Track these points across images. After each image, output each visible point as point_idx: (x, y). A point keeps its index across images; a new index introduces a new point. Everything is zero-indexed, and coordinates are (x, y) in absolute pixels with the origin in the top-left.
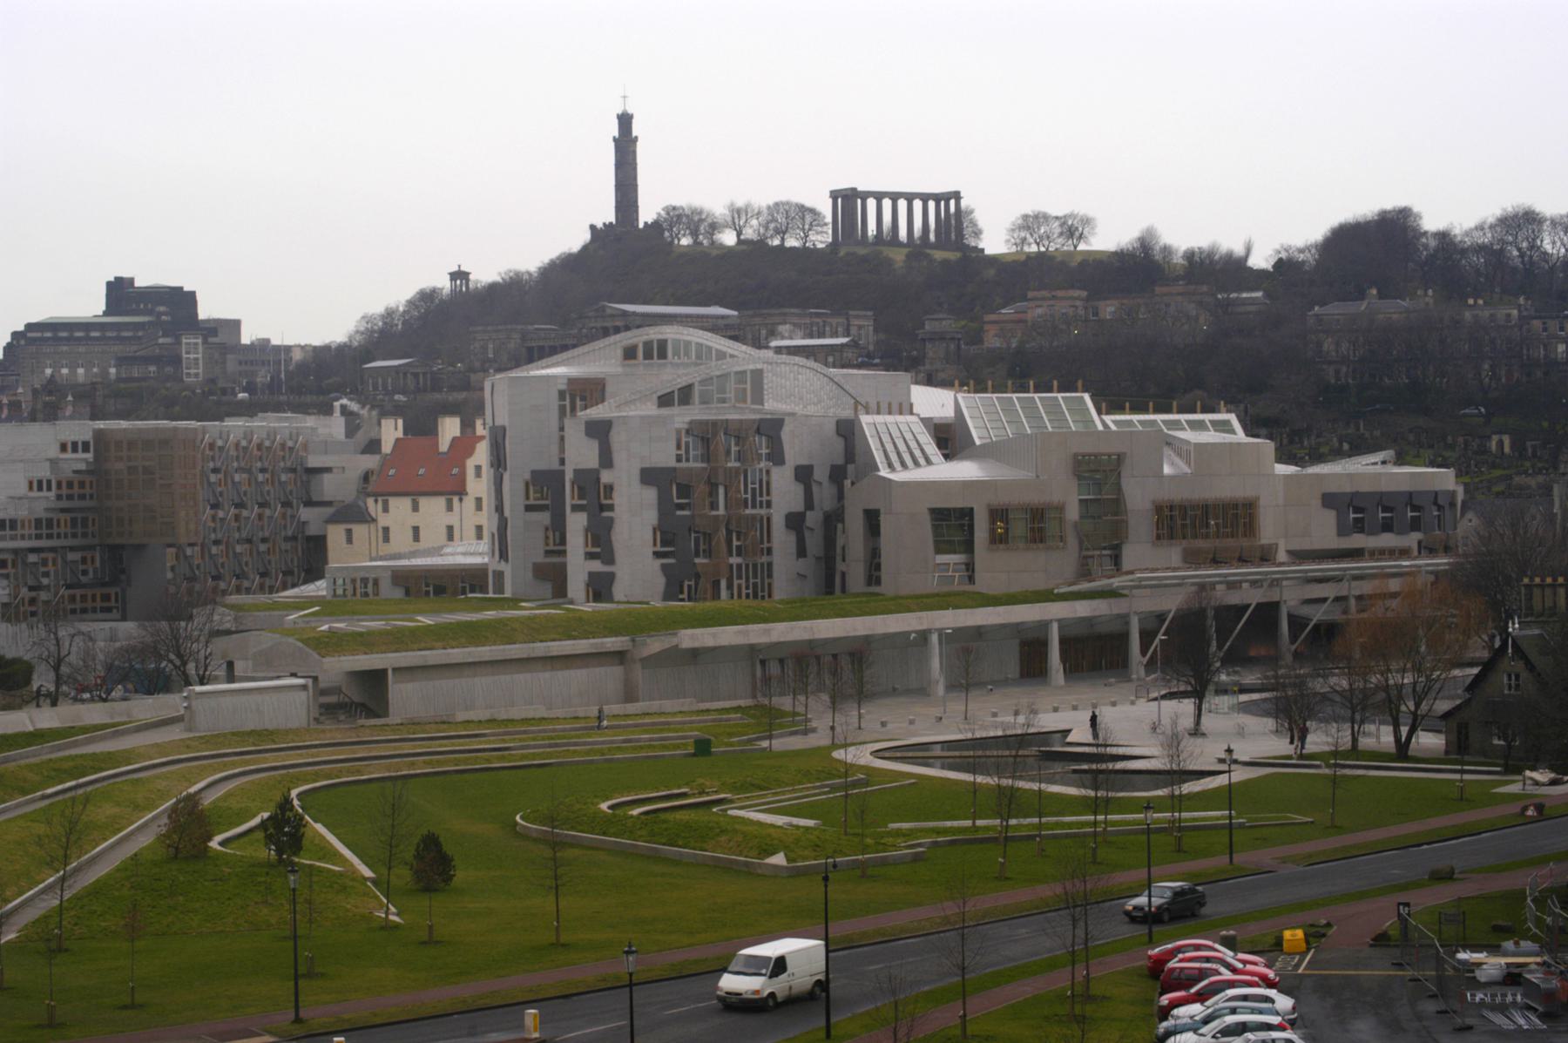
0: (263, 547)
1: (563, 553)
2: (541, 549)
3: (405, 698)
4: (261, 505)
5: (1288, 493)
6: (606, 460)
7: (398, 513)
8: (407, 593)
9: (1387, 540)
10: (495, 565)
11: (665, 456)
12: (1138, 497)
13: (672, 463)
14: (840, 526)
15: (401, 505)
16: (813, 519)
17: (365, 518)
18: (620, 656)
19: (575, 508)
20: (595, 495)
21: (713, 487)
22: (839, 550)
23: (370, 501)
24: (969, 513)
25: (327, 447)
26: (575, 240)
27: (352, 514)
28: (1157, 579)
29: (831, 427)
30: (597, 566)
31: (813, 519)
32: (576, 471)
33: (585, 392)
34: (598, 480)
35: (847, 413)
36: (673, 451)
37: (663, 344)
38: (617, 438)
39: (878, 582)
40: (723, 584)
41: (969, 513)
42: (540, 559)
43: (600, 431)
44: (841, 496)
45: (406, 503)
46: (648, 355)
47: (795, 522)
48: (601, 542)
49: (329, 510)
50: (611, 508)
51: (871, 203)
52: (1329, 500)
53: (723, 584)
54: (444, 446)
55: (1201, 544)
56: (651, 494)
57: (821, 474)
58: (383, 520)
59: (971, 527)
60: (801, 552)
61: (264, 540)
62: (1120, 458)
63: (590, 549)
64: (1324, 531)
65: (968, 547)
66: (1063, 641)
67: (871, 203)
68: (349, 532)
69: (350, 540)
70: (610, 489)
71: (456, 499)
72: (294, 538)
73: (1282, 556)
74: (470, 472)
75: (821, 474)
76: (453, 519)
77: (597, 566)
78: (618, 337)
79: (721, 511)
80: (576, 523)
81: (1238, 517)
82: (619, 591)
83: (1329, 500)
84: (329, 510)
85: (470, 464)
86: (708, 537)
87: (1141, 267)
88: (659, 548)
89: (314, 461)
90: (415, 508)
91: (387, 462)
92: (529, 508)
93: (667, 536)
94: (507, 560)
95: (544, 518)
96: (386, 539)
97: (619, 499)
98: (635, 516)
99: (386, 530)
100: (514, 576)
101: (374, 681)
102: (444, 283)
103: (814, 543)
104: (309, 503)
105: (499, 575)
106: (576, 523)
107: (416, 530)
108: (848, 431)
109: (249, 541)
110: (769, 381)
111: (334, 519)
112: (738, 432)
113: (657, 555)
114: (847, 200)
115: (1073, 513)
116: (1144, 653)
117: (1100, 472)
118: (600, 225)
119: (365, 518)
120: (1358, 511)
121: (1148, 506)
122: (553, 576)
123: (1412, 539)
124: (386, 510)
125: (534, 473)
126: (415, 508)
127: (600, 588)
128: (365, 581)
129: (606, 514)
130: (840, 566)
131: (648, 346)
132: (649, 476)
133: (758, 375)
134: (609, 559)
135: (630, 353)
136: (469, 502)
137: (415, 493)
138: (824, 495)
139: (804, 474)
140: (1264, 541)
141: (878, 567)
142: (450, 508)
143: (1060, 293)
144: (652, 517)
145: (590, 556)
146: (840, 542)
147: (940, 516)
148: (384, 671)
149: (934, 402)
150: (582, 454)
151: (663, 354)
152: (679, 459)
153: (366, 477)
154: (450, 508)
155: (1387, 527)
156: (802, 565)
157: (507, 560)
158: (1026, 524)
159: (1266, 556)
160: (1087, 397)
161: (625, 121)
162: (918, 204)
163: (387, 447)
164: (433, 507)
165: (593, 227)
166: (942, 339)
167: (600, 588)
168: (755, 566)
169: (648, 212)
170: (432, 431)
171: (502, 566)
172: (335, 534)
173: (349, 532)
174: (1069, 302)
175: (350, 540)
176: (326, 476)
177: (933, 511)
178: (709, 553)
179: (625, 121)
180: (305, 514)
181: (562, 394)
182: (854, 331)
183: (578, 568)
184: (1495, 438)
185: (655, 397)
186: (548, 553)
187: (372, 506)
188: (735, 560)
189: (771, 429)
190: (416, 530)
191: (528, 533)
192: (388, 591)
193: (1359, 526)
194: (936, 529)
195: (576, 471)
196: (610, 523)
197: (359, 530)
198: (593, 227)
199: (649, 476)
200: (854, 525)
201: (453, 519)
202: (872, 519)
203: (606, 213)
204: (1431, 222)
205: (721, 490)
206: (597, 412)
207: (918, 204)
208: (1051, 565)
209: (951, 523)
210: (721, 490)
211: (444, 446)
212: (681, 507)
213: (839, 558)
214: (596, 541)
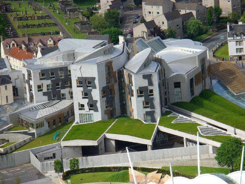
6: (151, 83)
19: (139, 96)
30: (149, 110)
32: (139, 88)
43: (148, 77)
50: (153, 95)
63: (145, 106)
70: (151, 91)
77: (149, 110)
94: (96, 110)
95: (105, 99)
125: (103, 88)
129: (151, 97)
134: (153, 107)
145: (145, 107)
186: (107, 107)
195: (139, 88)
202: (177, 85)
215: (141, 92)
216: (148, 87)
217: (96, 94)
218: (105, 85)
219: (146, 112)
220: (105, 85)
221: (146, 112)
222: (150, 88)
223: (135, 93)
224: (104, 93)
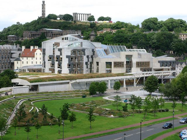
0: (6, 64)
1: (54, 67)
2: (50, 66)
3: (41, 89)
4: (5, 58)
5: (155, 62)
6: (61, 54)
7: (25, 60)
8: (30, 71)
9: (167, 67)
10: (42, 68)
11: (69, 54)
12: (134, 60)
13: (70, 55)
14: (93, 65)
15: (25, 58)
16: (89, 63)
17: (20, 60)
18: (68, 83)
19: (57, 61)
20: (59, 59)
21: (76, 58)
22: (92, 67)
23: (21, 58)
24: (111, 63)
25: (14, 50)
26: (36, 18)
27: (18, 60)
28: (136, 73)
29: (91, 50)
31: (89, 63)
33: (57, 44)
34: (60, 57)
35: (93, 48)
36: (70, 53)
37: (67, 38)
38: (63, 51)
39: (98, 72)
40: (77, 72)
41: (111, 63)
42: (50, 67)
43: (60, 50)
44: (93, 60)
45: (26, 58)
46: (65, 39)
47: (86, 63)
48: (60, 66)
49: (15, 59)
50: (62, 61)
51: (78, 15)
52: (159, 62)
53: (77, 72)
54: (31, 50)
55: (142, 67)
56: (68, 59)
57: (90, 57)
58: (22, 61)
59: (111, 65)
60: (87, 67)
61: (6, 63)
62: (131, 56)
64: (158, 66)
65: (111, 67)
66: (126, 81)
67: (78, 15)
68: (17, 62)
69: (18, 63)
70: (61, 58)
71: (33, 58)
72: (9, 63)
73: (153, 70)
74: (35, 54)
75: (90, 57)
76: (32, 61)
77: (59, 69)
78: (61, 37)
79: (77, 62)
80: (56, 63)
81: (148, 63)
82: (62, 72)
83: (159, 62)
84: (15, 59)
85: (35, 53)
86: (75, 65)
87: (119, 26)
88: (68, 67)
89: (12, 52)
90: (27, 59)
91: (23, 52)
92: (48, 60)
93: (69, 65)
95: (51, 62)
96: (23, 63)
97: (63, 60)
98: (65, 62)
99: (23, 62)
100: (47, 70)
101: (37, 86)
102: (16, 24)
103: (89, 66)
104: (12, 58)
105: (44, 70)
106: (56, 63)
107: (27, 62)
108: (93, 51)
109: (3, 63)
110: (83, 44)
111: (15, 60)
112: (79, 51)
113: (69, 68)
114: (75, 14)
115: (125, 63)
116: (136, 83)
117: (129, 57)
118: (40, 17)
119: (20, 60)
120: (163, 63)
121: (136, 62)
122: (53, 71)
123: (170, 67)
124: (23, 59)
126: (27, 59)
127: (60, 72)
128: (24, 70)
130: (92, 70)
131: (65, 38)
132: (67, 57)
133: (82, 43)
135: (63, 39)
136: (35, 58)
137: (27, 57)
138: (90, 60)
139: (88, 57)
140: (151, 67)
141: (98, 70)
142: (32, 59)
143: (108, 29)
144: (68, 62)
145: (58, 67)
146: (93, 66)
147: (107, 63)
148: (38, 85)
149: (106, 47)
150: (57, 53)
151: (67, 39)
152: (71, 54)
153: (20, 54)
154: (32, 59)
155: (167, 66)
156: (87, 69)
157: (45, 68)
158: (118, 64)
159: (150, 70)
160: (125, 46)
161: (44, 2)
162: (85, 15)
163: (23, 50)
164: (30, 59)
165: (39, 17)
166: (93, 35)
167: (60, 72)
168: (81, 69)
169: (46, 15)
170: (30, 48)
171: (44, 68)
172: (15, 62)
173: (17, 62)
174: (109, 30)
175: (18, 63)
176: (14, 54)
177: (106, 62)
178: (75, 67)
179: (44, 2)
180: (11, 59)
181: (54, 44)
182: (78, 33)
183: (57, 69)
184: (171, 51)
185: (67, 46)
187: (21, 58)
188: (78, 68)
189: (84, 50)
190: (27, 62)
191: (48, 64)
192: (27, 71)
193: (163, 66)
194: (106, 65)
196: (61, 63)
197: (19, 62)
198: (39, 17)
199: (67, 57)
200: (95, 64)
201: (32, 61)
202: (98, 63)
203: (41, 15)
204: (159, 20)
205: (77, 59)
206: (60, 47)
207: (85, 15)
208: (123, 70)
209: (109, 64)
210: (77, 59)
211: (31, 50)
212: (71, 61)
213: (92, 69)
214: (59, 66)
215: (57, 59)
216: (60, 56)
217: (47, 58)
218: (52, 54)
219: (58, 70)
220: (52, 54)
221: (58, 70)
222: (61, 56)
223: (55, 59)
224: (50, 58)
